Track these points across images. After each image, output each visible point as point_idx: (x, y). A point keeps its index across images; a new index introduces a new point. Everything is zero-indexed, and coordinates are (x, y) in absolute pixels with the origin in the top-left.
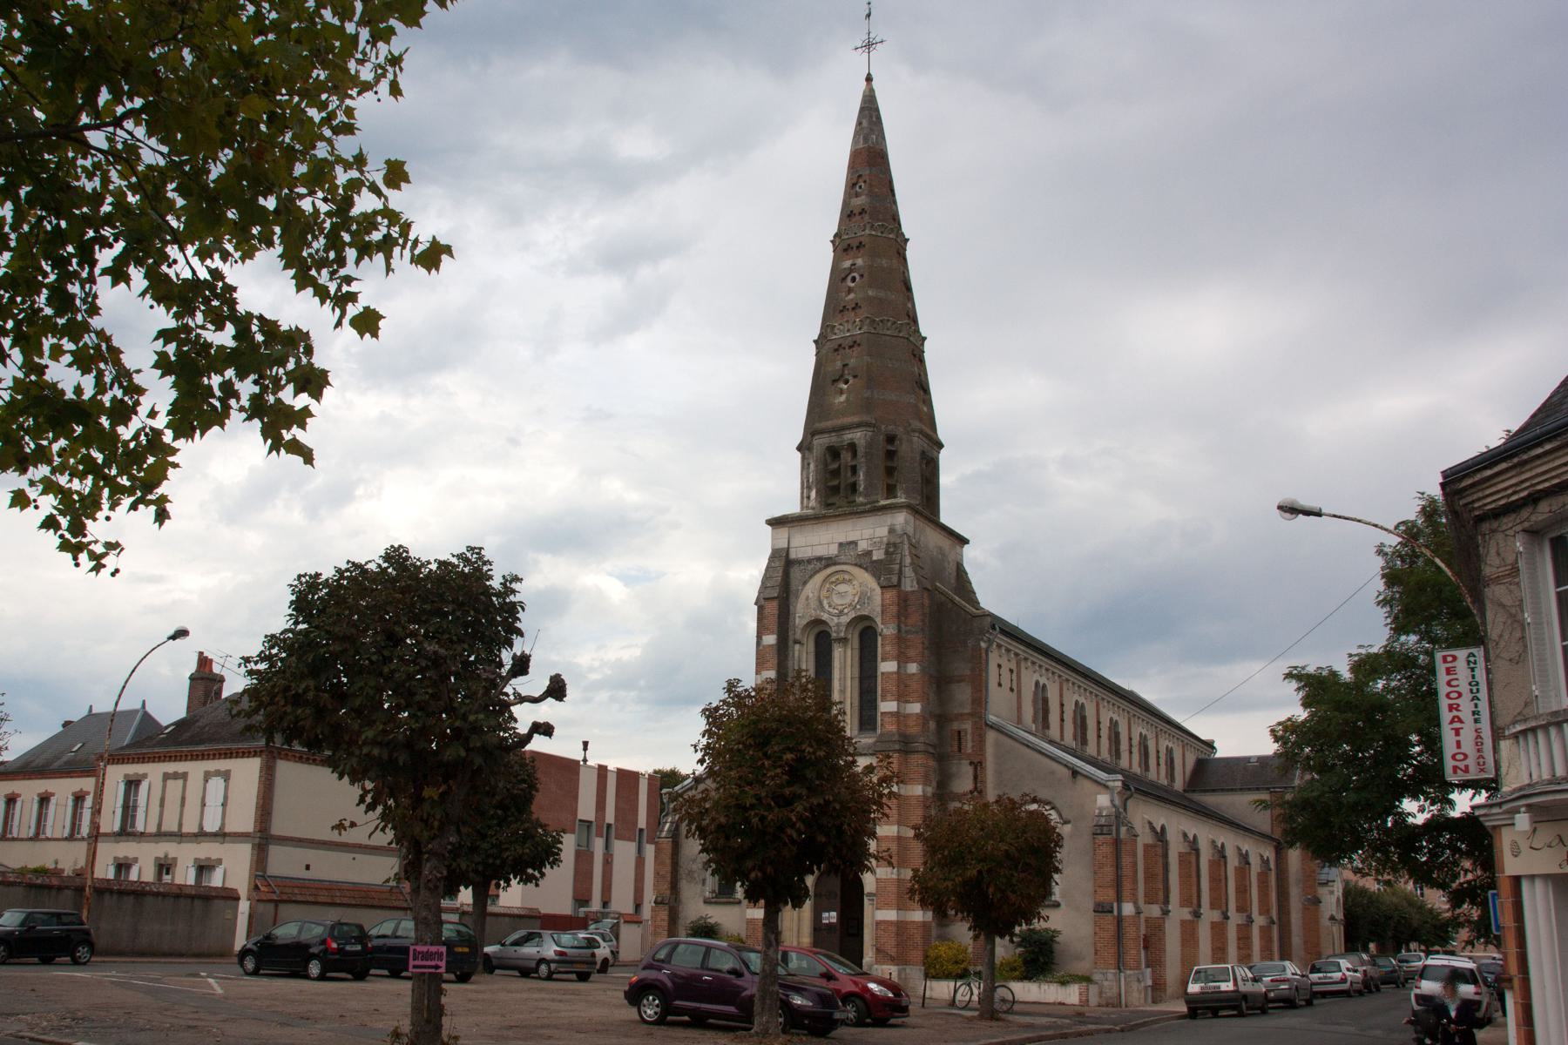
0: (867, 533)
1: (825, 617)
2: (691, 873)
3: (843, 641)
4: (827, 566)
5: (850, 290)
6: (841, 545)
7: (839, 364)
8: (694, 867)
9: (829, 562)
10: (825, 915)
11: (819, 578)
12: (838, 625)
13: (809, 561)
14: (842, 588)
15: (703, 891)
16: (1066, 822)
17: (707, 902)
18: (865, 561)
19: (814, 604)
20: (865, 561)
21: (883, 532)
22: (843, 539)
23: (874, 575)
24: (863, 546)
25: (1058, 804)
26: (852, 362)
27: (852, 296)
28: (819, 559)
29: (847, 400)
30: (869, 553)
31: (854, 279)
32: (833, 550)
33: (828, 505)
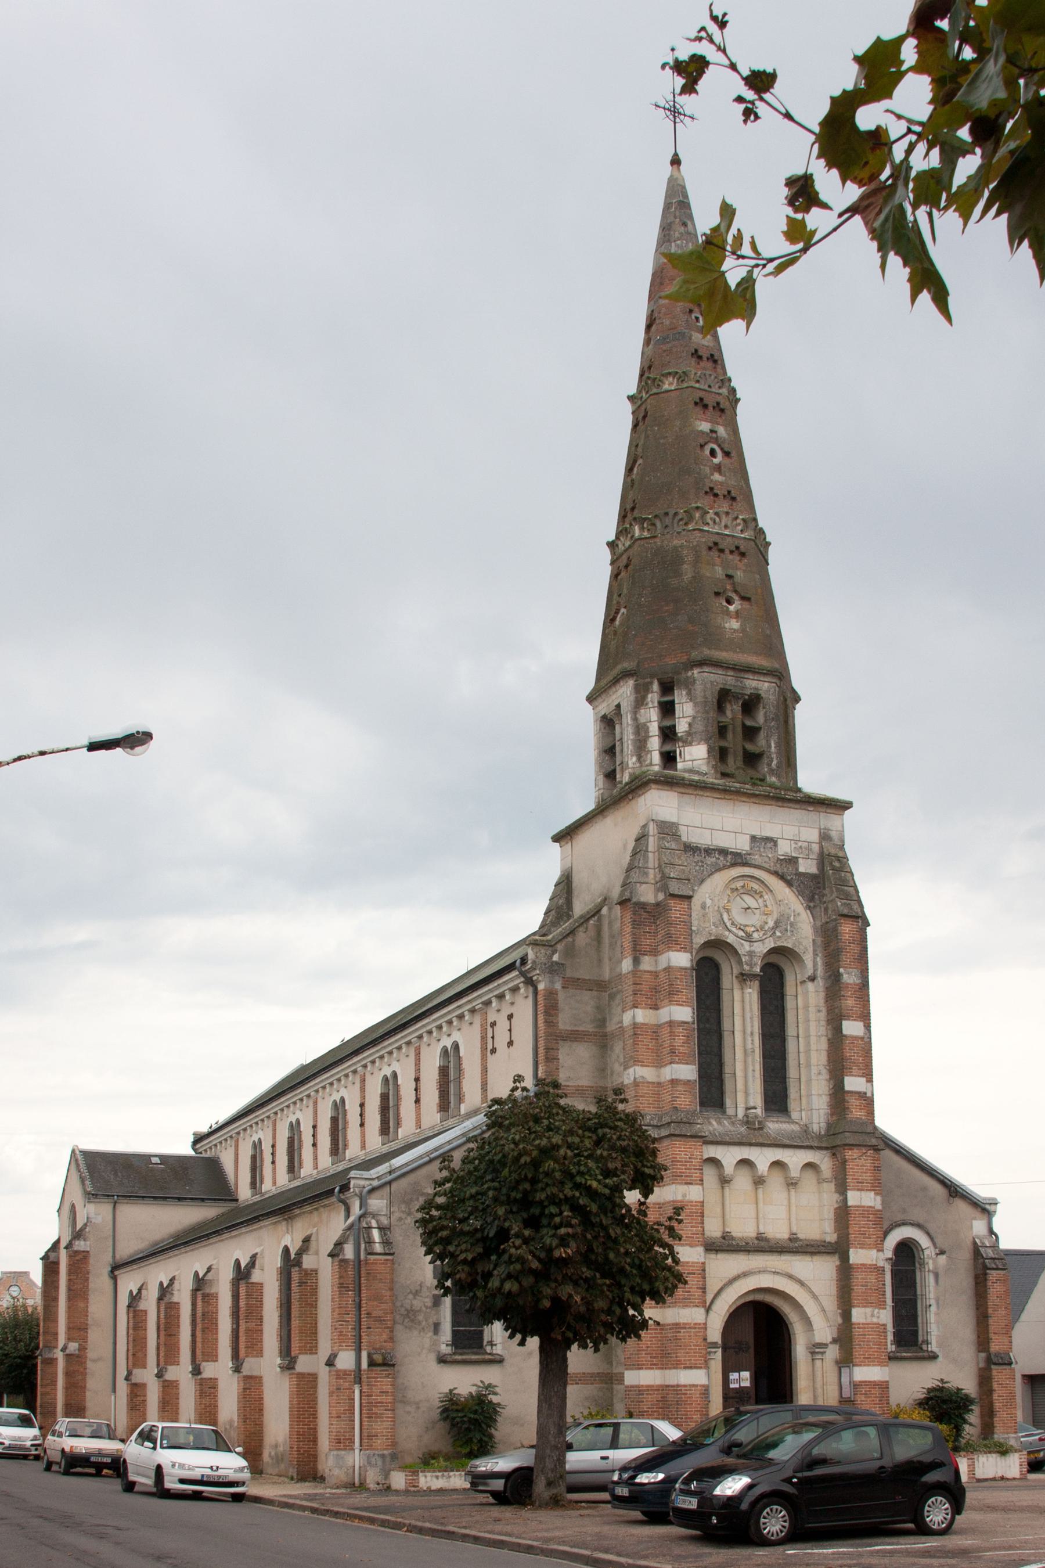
0: (790, 831)
1: (731, 939)
2: (410, 1315)
3: (744, 978)
4: (734, 865)
5: (718, 468)
6: (753, 838)
7: (719, 572)
8: (417, 1303)
9: (738, 859)
10: (733, 1376)
11: (720, 879)
12: (751, 954)
13: (708, 851)
14: (750, 901)
15: (435, 1343)
16: (942, 1252)
17: (442, 1360)
18: (786, 871)
19: (712, 917)
20: (786, 871)
21: (811, 835)
22: (757, 833)
23: (801, 893)
24: (784, 848)
25: (931, 1227)
26: (739, 575)
27: (717, 477)
28: (723, 852)
29: (743, 630)
30: (793, 861)
31: (713, 453)
32: (742, 844)
33: (724, 775)
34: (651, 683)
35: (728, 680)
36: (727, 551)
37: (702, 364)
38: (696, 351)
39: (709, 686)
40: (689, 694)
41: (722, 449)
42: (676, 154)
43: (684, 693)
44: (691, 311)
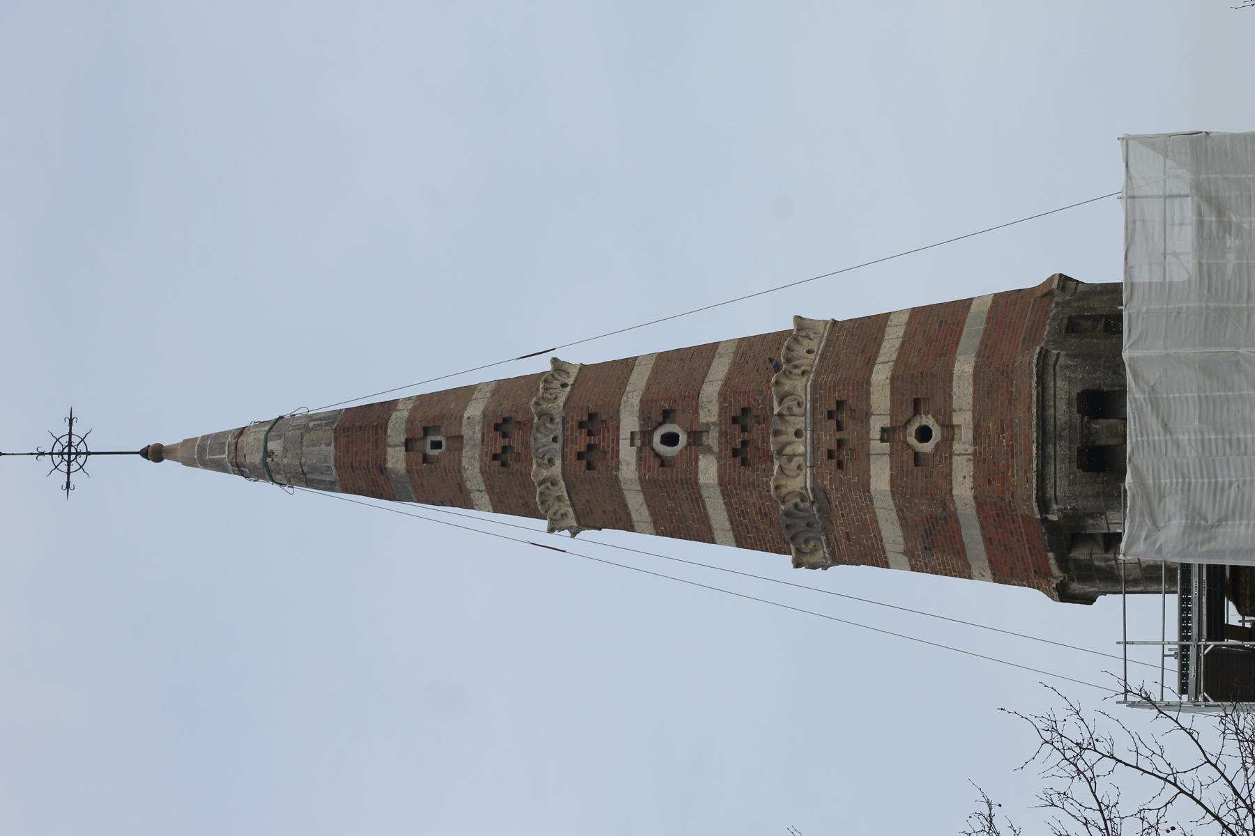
31: (670, 440)
34: (1076, 561)
35: (1062, 450)
36: (840, 435)
37: (518, 448)
38: (495, 457)
39: (1077, 489)
40: (1092, 516)
41: (660, 424)
42: (145, 453)
43: (1091, 522)
44: (425, 459)
